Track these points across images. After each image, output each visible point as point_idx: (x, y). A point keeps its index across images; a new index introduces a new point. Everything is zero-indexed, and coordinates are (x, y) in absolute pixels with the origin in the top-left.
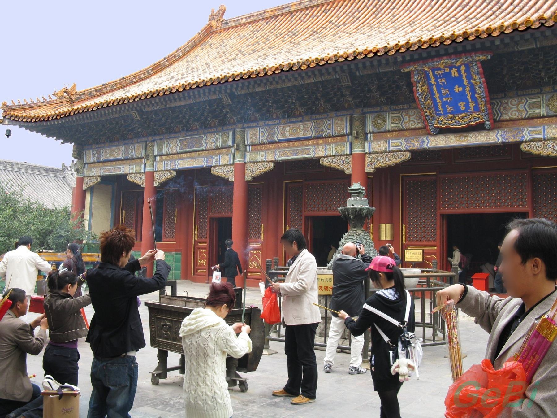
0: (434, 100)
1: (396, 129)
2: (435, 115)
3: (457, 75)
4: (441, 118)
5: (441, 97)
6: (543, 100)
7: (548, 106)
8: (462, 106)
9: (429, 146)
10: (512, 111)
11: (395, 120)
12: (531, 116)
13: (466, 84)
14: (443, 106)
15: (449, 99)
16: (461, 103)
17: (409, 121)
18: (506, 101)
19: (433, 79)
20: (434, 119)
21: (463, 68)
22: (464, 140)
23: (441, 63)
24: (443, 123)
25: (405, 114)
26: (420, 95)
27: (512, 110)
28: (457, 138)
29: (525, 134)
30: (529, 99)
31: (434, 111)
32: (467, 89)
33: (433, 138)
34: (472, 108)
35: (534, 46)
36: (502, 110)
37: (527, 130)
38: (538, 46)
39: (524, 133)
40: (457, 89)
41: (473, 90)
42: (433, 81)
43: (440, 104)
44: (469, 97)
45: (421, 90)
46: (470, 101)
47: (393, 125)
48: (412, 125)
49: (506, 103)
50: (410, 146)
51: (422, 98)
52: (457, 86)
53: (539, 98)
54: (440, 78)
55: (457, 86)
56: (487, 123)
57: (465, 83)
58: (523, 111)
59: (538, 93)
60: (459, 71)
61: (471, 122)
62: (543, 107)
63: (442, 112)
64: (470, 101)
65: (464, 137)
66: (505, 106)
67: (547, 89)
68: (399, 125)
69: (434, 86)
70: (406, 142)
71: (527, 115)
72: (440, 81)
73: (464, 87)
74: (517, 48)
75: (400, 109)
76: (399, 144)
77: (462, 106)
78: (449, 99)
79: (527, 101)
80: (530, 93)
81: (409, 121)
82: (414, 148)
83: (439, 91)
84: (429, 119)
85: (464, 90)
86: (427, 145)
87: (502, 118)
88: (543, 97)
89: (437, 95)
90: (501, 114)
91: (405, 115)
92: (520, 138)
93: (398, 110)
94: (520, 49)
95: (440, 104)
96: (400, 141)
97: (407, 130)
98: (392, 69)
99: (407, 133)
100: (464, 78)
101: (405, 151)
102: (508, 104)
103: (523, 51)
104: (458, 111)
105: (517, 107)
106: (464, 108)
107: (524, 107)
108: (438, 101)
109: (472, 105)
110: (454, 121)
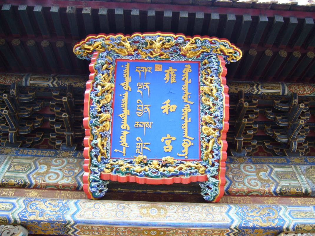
0: (116, 121)
1: (13, 182)
2: (108, 155)
3: (173, 80)
4: (120, 162)
5: (131, 120)
6: (297, 170)
7: (309, 178)
8: (168, 142)
9: (77, 218)
10: (250, 179)
11: (17, 168)
12: (285, 189)
13: (186, 101)
14: (130, 138)
15: (146, 124)
16: (169, 136)
17: (47, 172)
18: (236, 165)
19: (128, 80)
20: (104, 161)
21: (188, 69)
22: (159, 216)
23: (158, 39)
24: (123, 169)
25: (42, 161)
26: (96, 95)
27: (249, 177)
28: (144, 211)
29: (284, 215)
30: (275, 167)
31: (109, 147)
32: (186, 110)
33: (90, 204)
34: (186, 150)
35: (280, 91)
36: (231, 176)
37: (286, 209)
38: (286, 93)
39: (281, 213)
40: (168, 107)
41: (196, 113)
42: (126, 85)
43: (125, 133)
44: (186, 126)
45: (103, 87)
46: (186, 135)
47: (9, 174)
48: (52, 180)
49: (236, 168)
50: (31, 214)
51: (98, 102)
52: (168, 101)
53: (291, 167)
54: (143, 80)
55: (168, 101)
56: (213, 180)
57: (185, 98)
58: (268, 180)
59: (283, 163)
60: (179, 75)
61: (182, 174)
62: (302, 179)
63: (124, 152)
64: (186, 135)
65: (159, 209)
66: (236, 171)
67: (297, 160)
68: (25, 176)
69: (126, 94)
70: (26, 205)
71: (279, 188)
72: (140, 85)
73: (181, 104)
74: (257, 87)
75: (36, 156)
76: (10, 207)
77: (168, 142)
78: (146, 124)
79: (272, 170)
80: (272, 161)
81: (47, 172)
82: (40, 219)
83: (132, 106)
84: (96, 156)
85: (179, 111)
86: (73, 216)
87: (234, 189)
88: (295, 167)
89: (126, 112)
90: (231, 182)
91: (40, 164)
92: (277, 221)
93: (32, 155)
94: (261, 91)
95: (125, 133)
96: (14, 201)
97: (36, 187)
98: (50, 83)
99: (33, 193)
100: (186, 87)
101: (15, 224)
102: (239, 169)
103: (262, 96)
104: (156, 152)
105: (258, 174)
106: (171, 147)
107: (269, 175)
108: (125, 125)
109: (186, 145)
110: (147, 168)
